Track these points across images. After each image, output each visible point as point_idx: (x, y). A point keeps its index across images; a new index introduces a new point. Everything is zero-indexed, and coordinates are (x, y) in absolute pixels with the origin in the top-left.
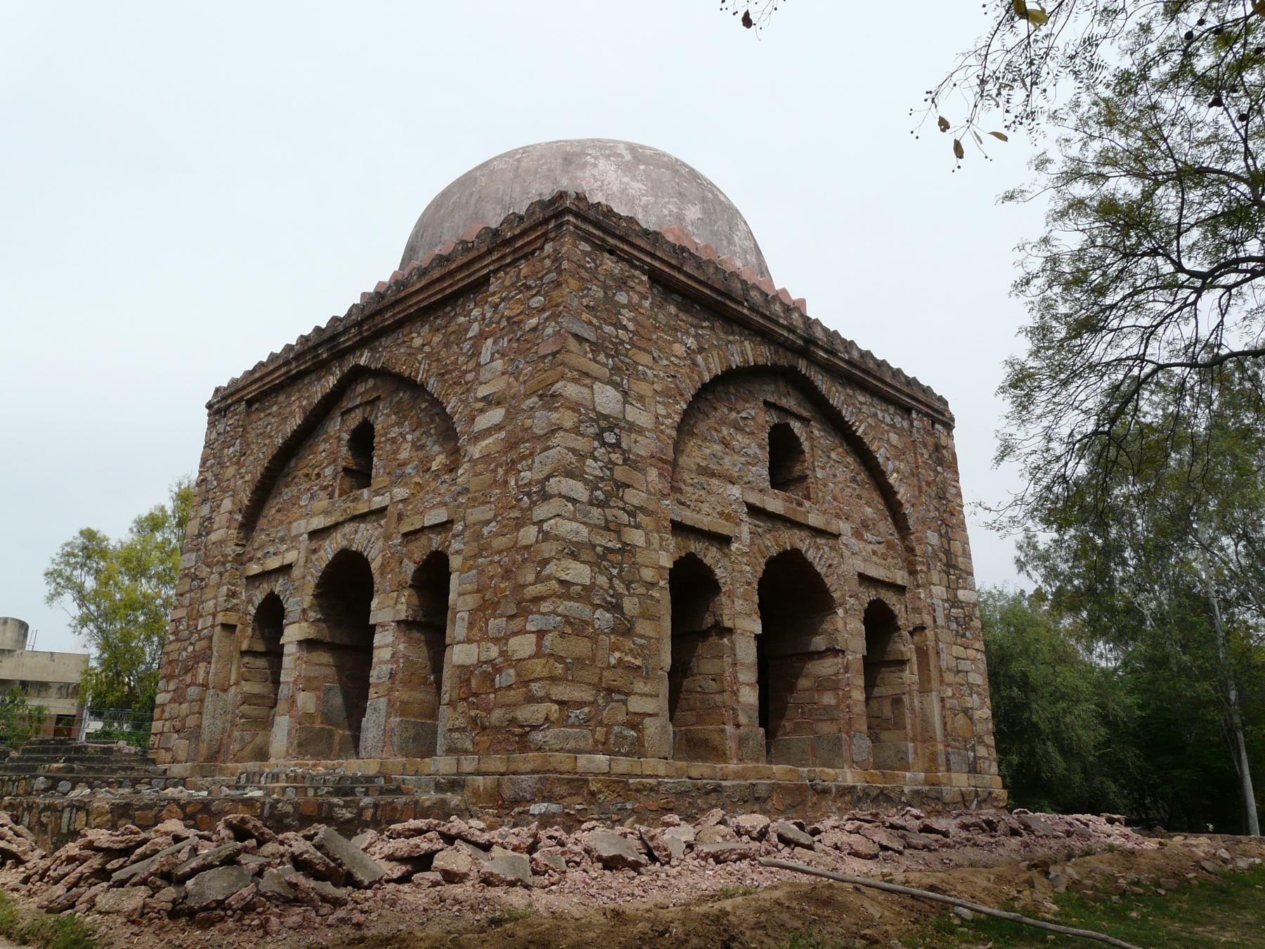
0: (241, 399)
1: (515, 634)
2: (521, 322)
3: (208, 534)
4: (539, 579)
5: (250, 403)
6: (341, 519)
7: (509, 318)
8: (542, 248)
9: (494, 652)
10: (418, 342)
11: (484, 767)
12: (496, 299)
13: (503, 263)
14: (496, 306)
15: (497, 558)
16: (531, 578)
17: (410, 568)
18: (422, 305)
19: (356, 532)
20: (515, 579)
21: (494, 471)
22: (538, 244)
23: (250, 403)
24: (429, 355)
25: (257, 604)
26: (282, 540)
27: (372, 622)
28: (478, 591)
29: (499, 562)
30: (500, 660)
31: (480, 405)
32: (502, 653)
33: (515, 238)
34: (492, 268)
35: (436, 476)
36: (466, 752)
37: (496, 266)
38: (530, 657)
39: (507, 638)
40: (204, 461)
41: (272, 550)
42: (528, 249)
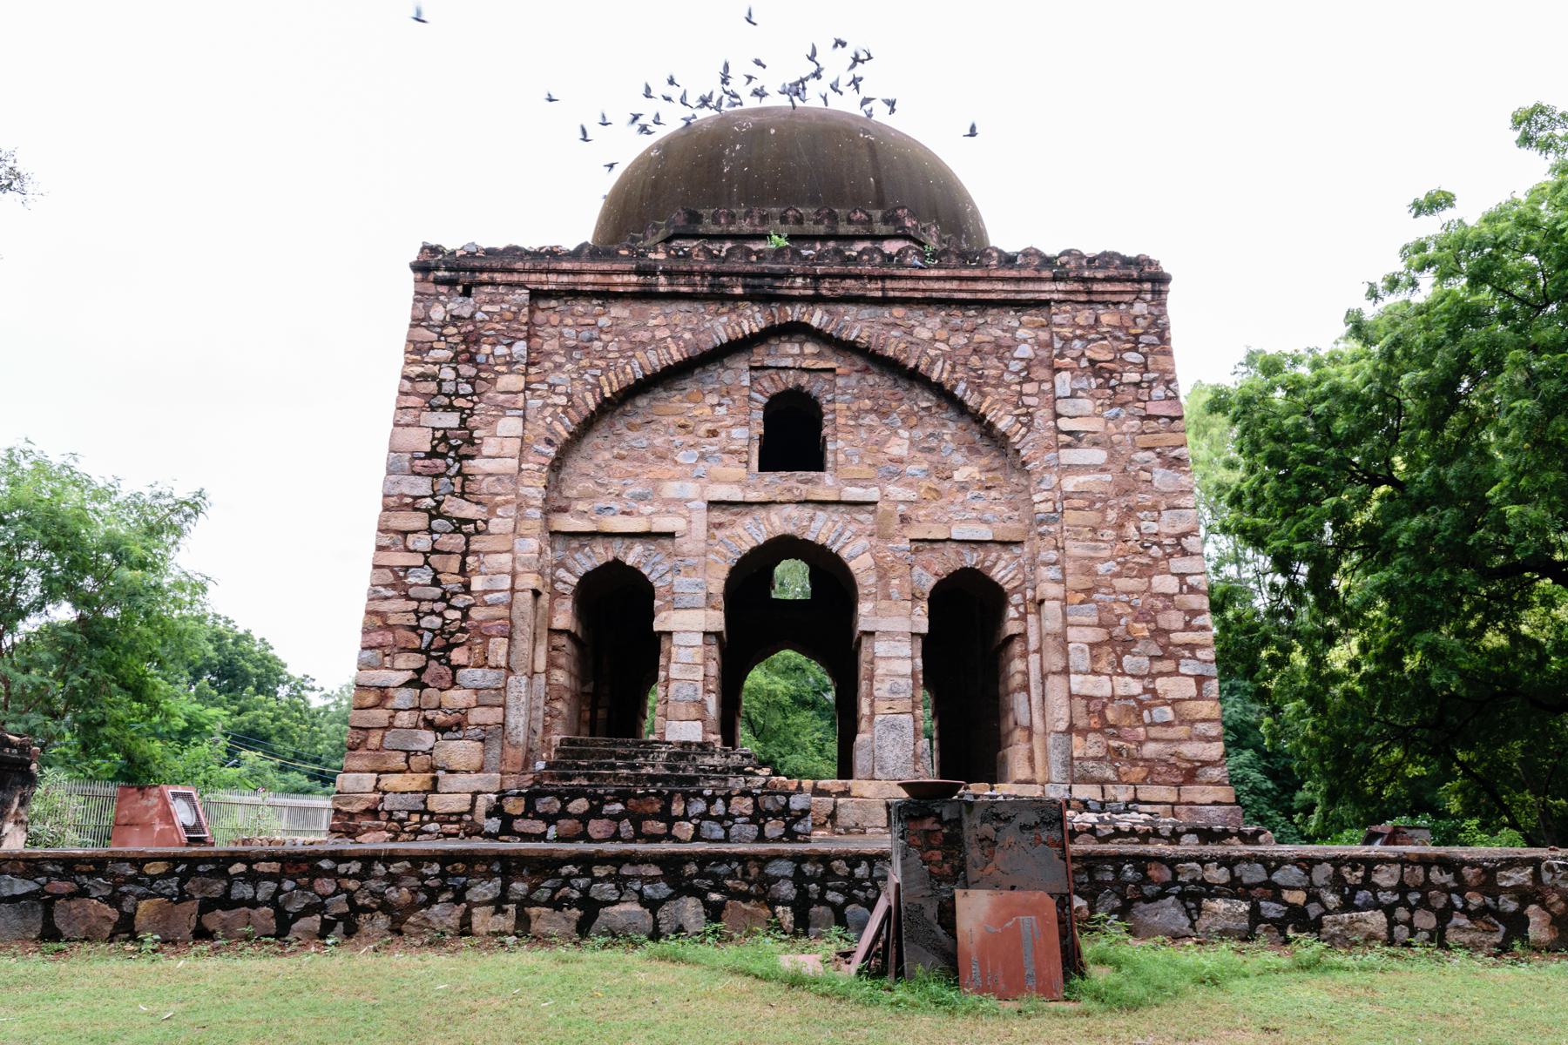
0: (521, 285)
1: (1161, 674)
2: (1111, 372)
3: (460, 458)
4: (1188, 627)
5: (536, 295)
6: (780, 498)
7: (1092, 362)
8: (1131, 304)
9: (1136, 687)
10: (923, 334)
11: (1141, 796)
12: (1066, 332)
13: (1072, 297)
14: (1066, 341)
15: (1124, 598)
16: (1181, 625)
17: (929, 582)
18: (934, 295)
19: (812, 519)
20: (1156, 622)
21: (1103, 511)
22: (1127, 298)
23: (536, 295)
24: (945, 356)
25: (581, 571)
26: (641, 498)
27: (863, 625)
28: (1100, 625)
29: (1128, 603)
30: (1148, 696)
31: (1067, 439)
32: (1146, 690)
33: (1094, 280)
34: (1055, 296)
35: (963, 487)
36: (1108, 781)
37: (1061, 296)
38: (1190, 699)
39: (1153, 676)
40: (417, 349)
41: (617, 506)
42: (1115, 298)
